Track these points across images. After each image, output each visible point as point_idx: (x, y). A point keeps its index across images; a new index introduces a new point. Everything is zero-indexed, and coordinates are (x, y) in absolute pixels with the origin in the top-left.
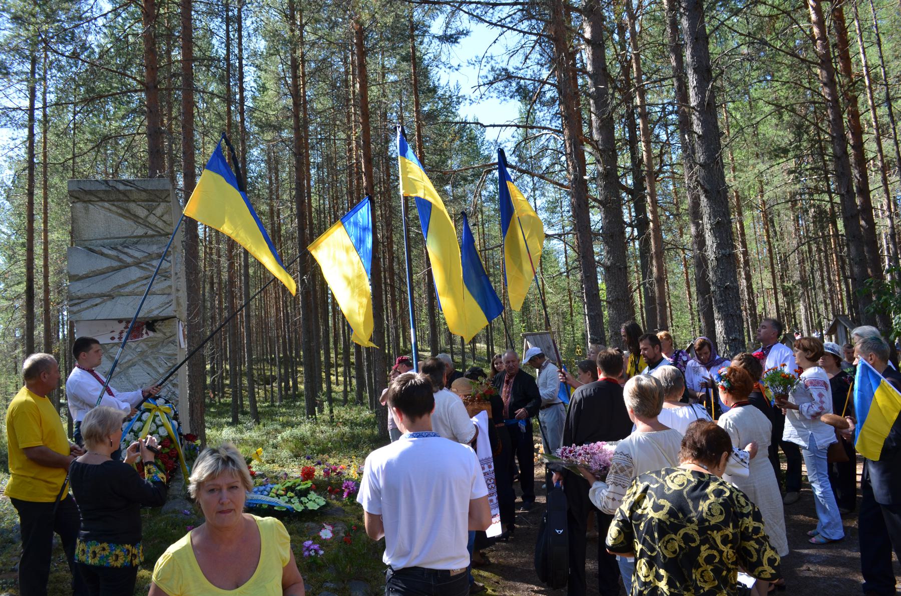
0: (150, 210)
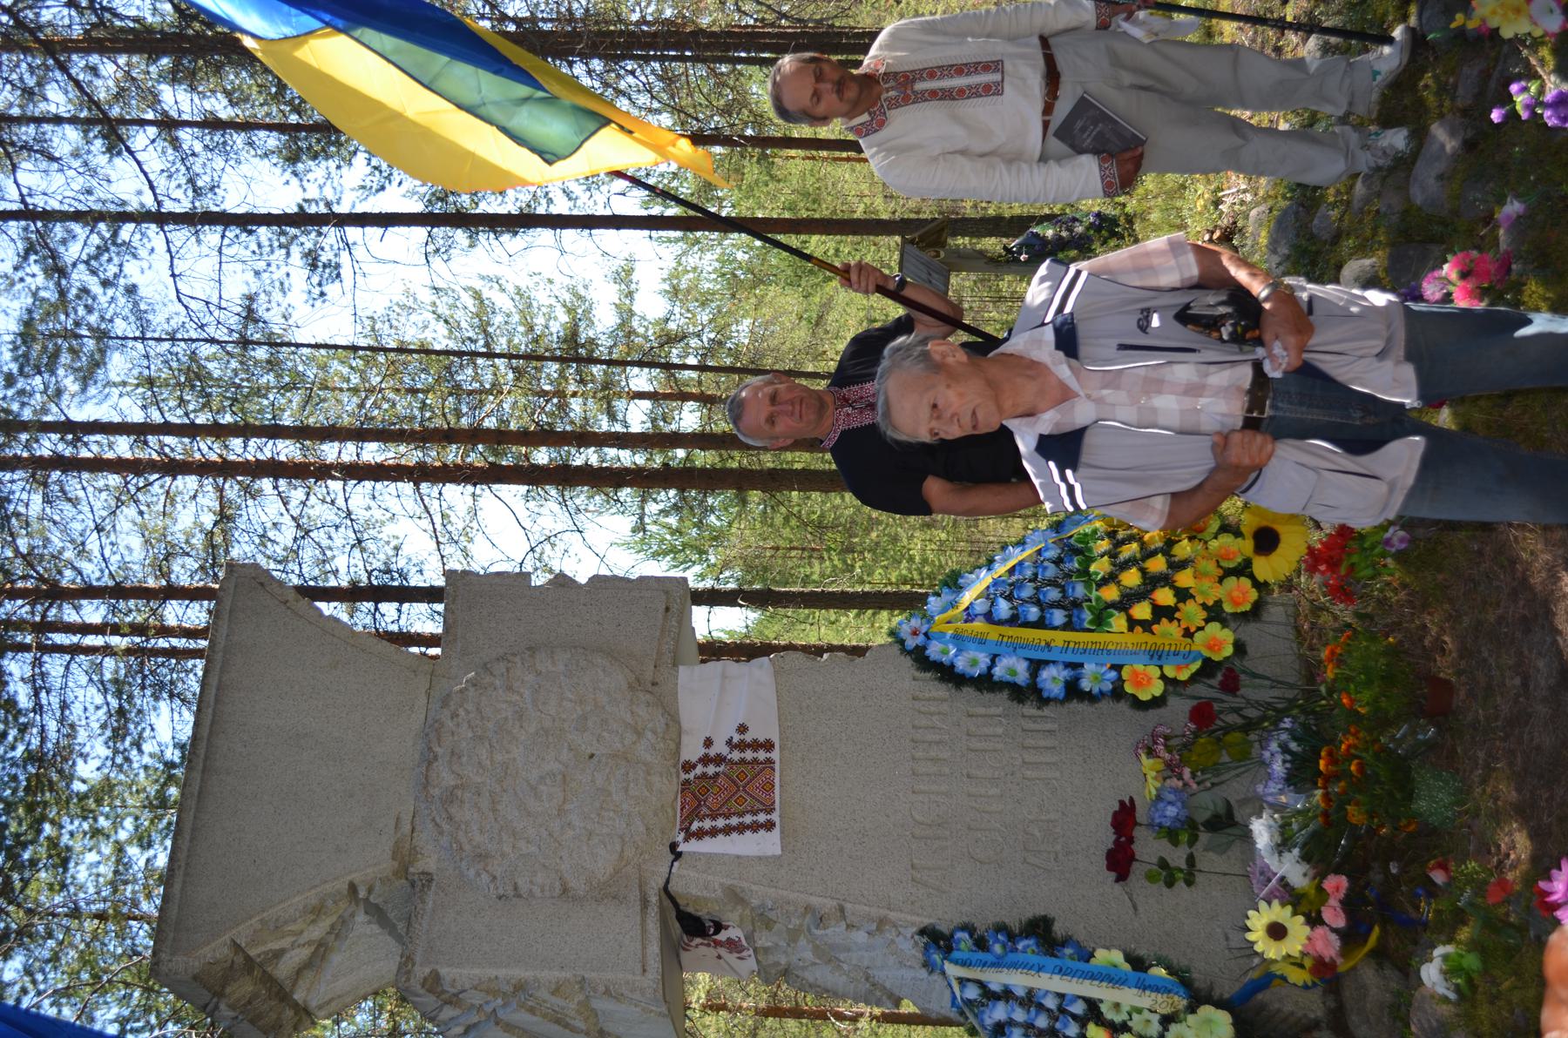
0: (278, 954)
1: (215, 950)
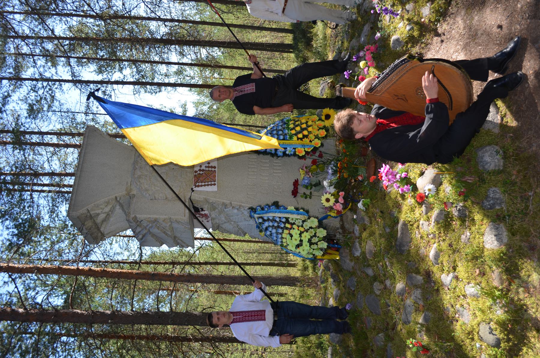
0: (98, 215)
1: (83, 211)
